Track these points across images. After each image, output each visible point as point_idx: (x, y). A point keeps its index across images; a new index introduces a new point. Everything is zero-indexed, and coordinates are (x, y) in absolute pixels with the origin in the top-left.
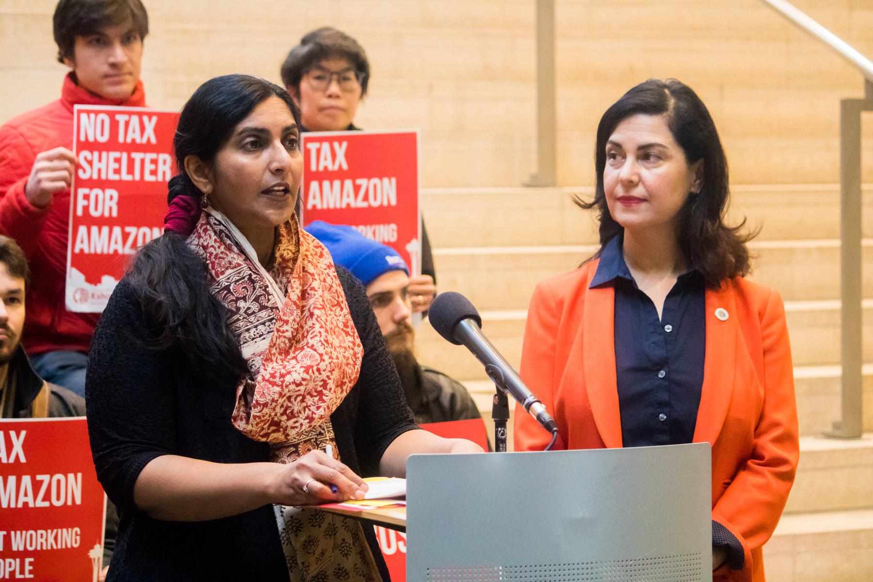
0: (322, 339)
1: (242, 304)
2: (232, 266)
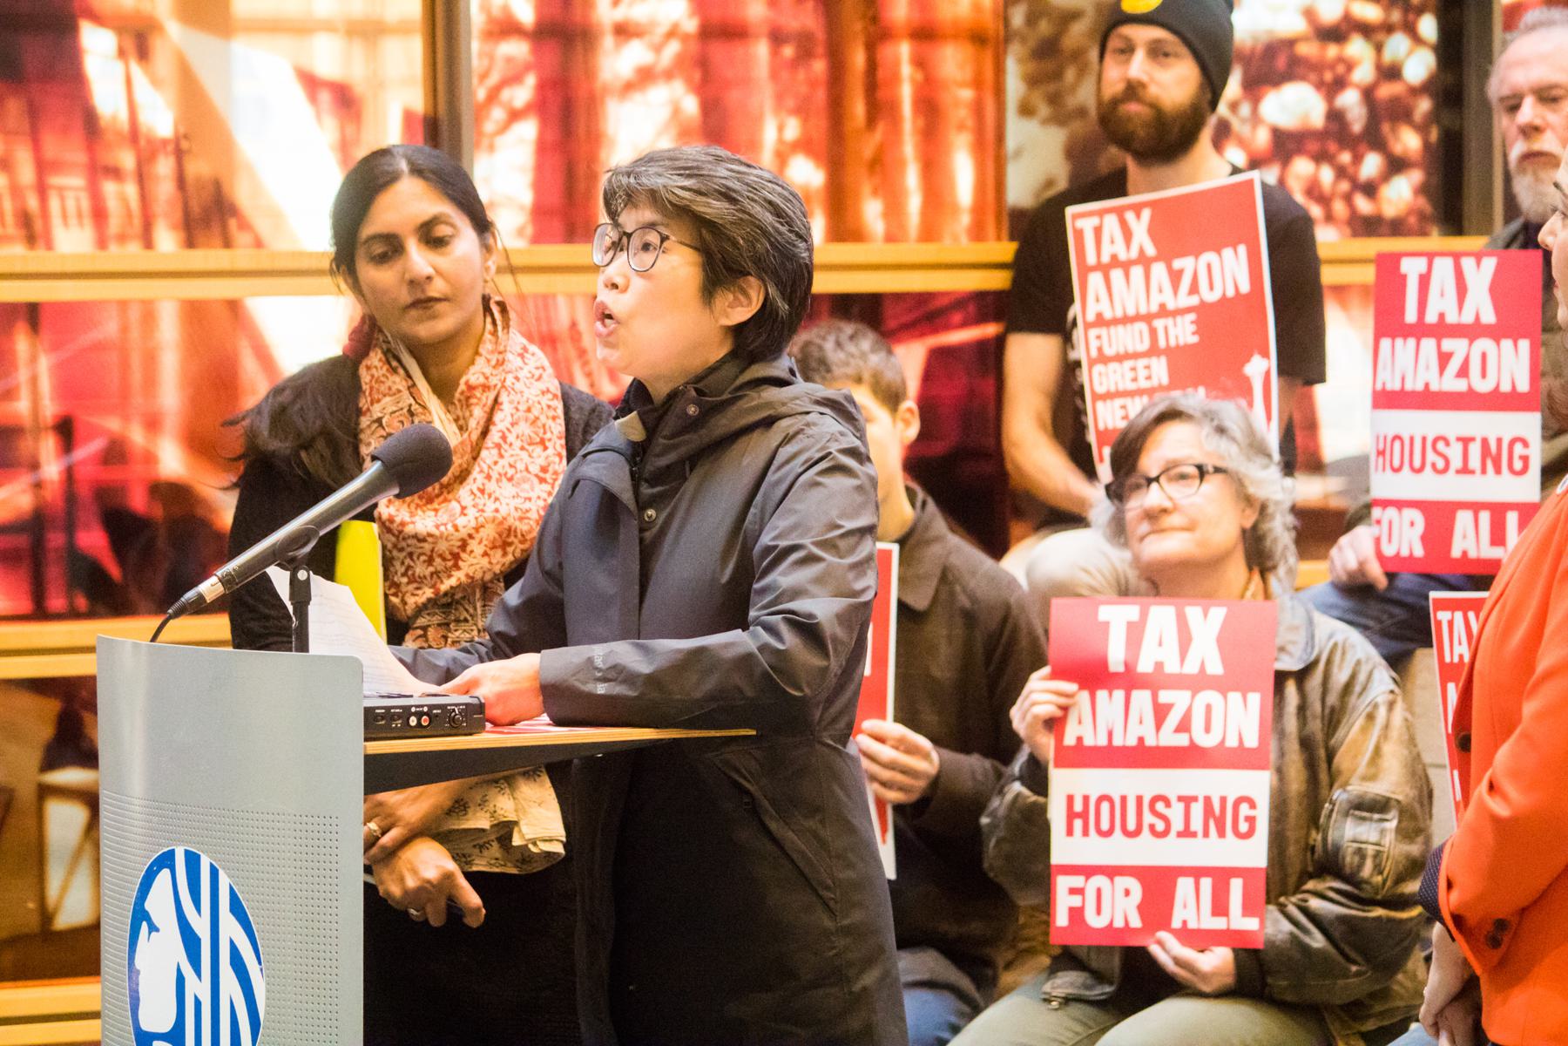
2: (391, 393)
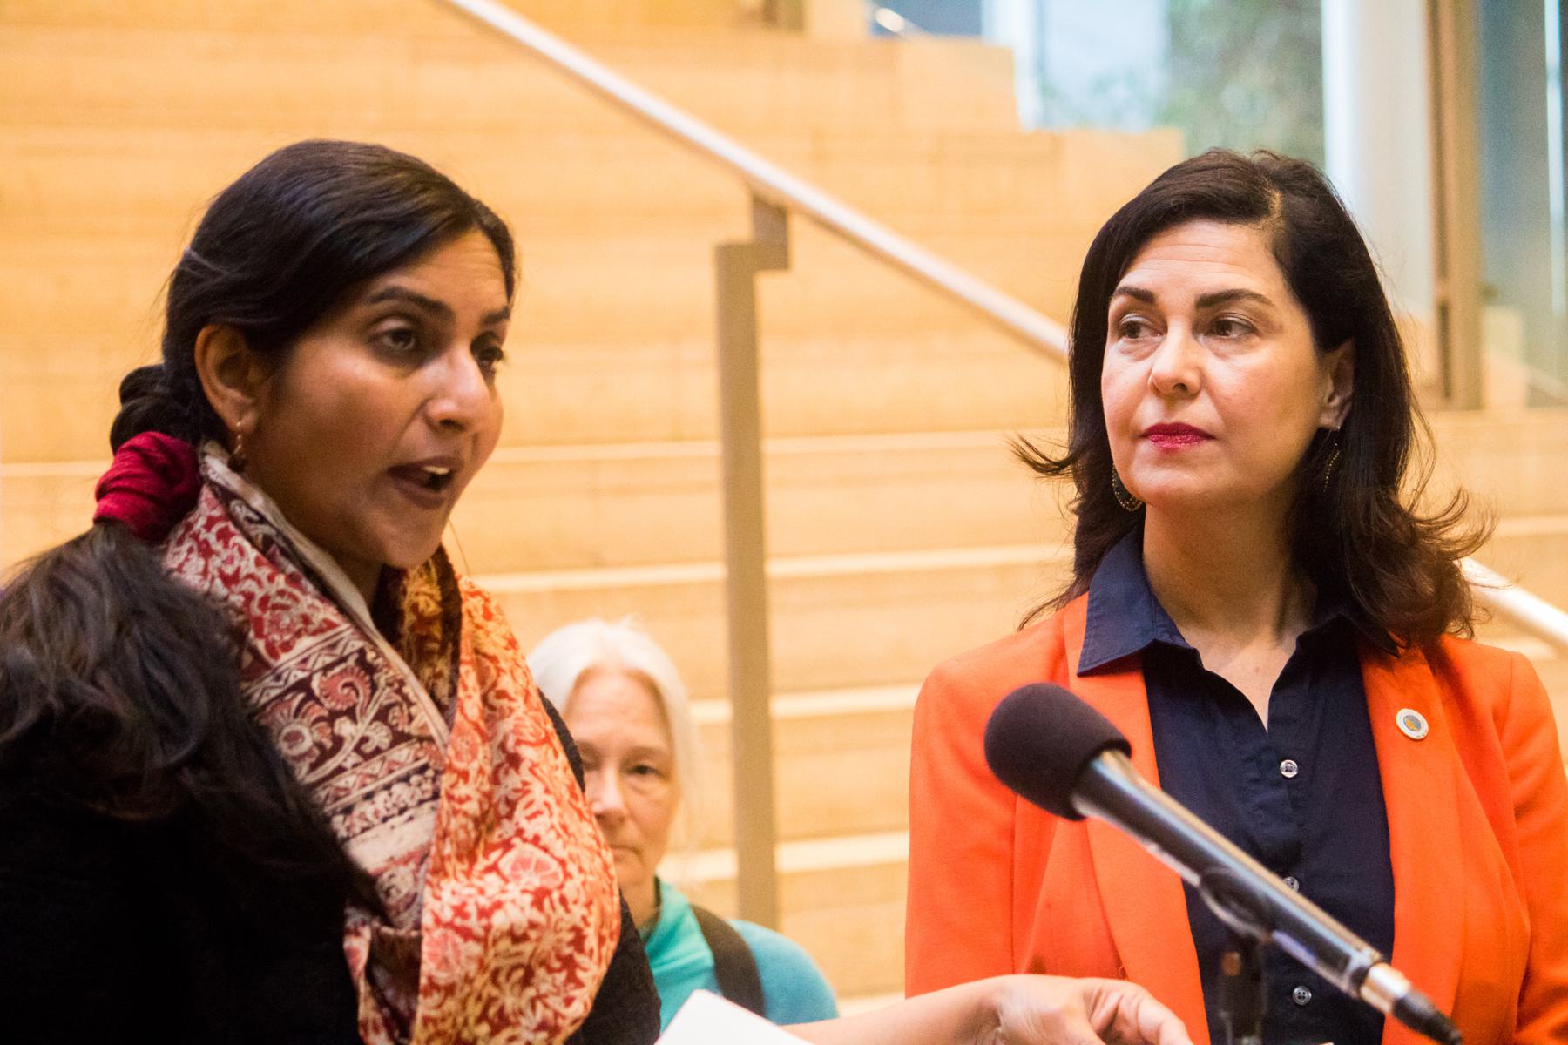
0: (555, 820)
1: (345, 727)
2: (311, 628)
